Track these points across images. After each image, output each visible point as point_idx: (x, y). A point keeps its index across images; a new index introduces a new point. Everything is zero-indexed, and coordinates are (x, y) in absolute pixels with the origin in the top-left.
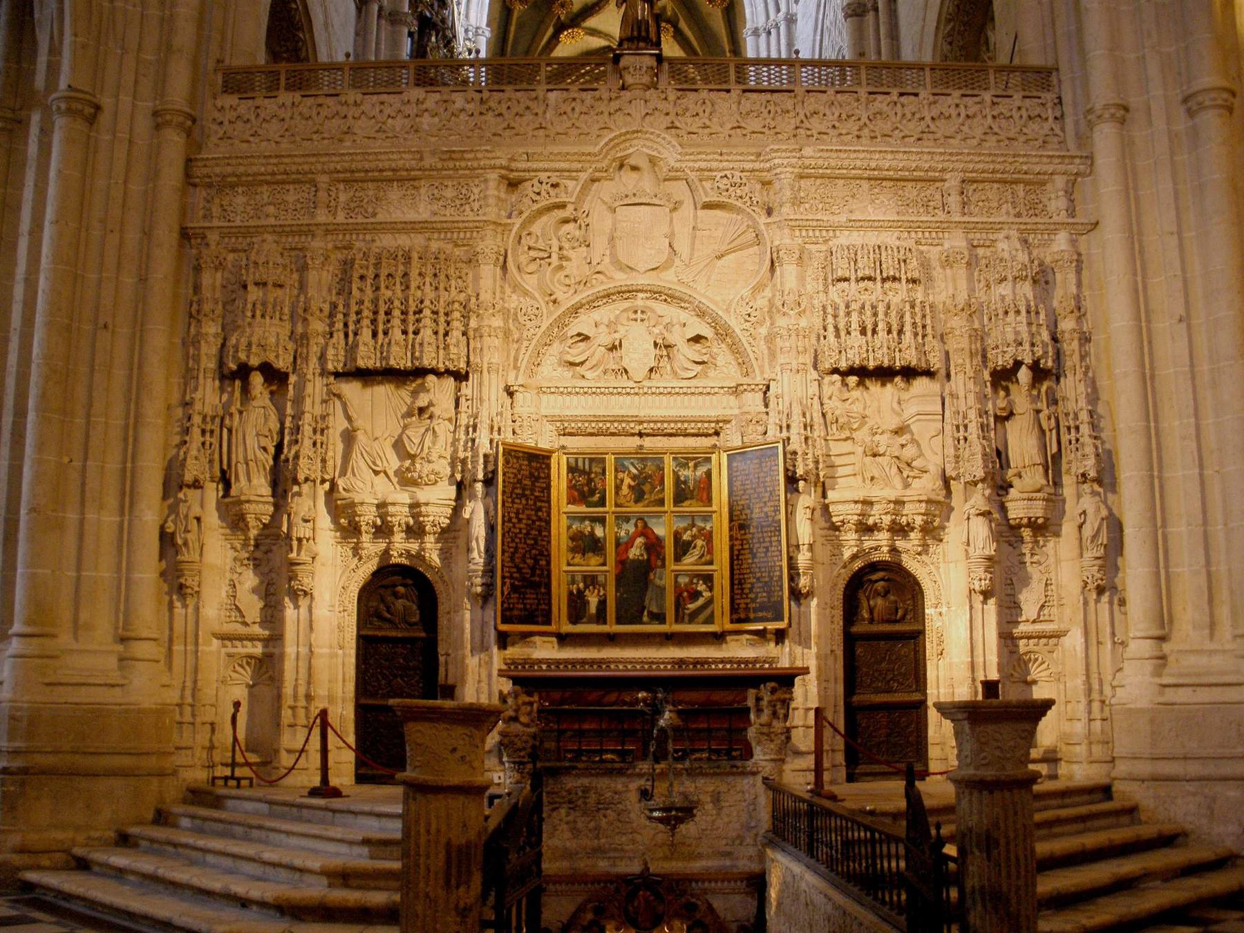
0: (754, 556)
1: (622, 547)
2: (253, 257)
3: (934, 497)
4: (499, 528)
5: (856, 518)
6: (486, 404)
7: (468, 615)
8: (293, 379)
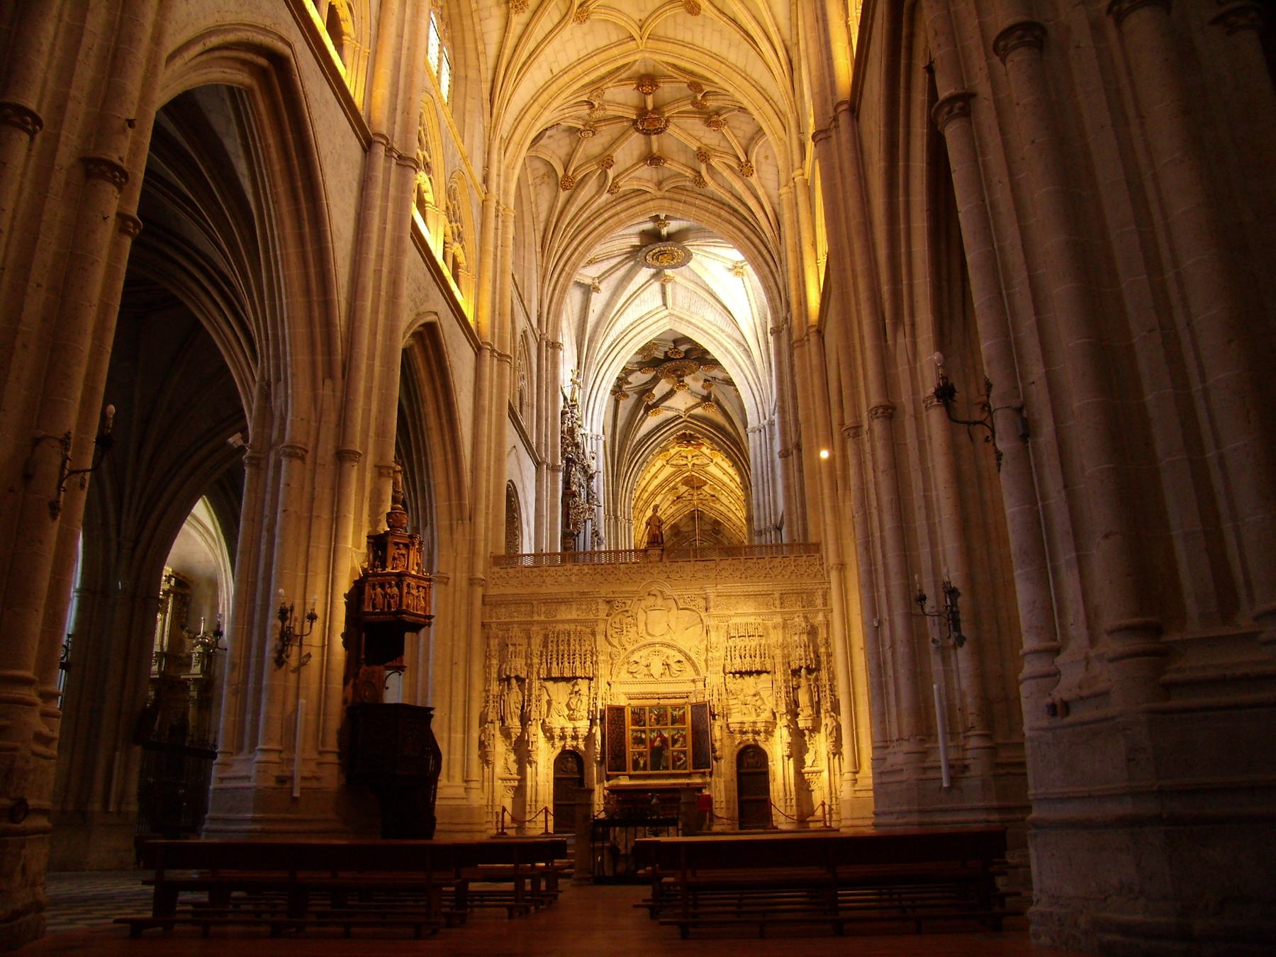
3: (768, 720)
8: (527, 681)
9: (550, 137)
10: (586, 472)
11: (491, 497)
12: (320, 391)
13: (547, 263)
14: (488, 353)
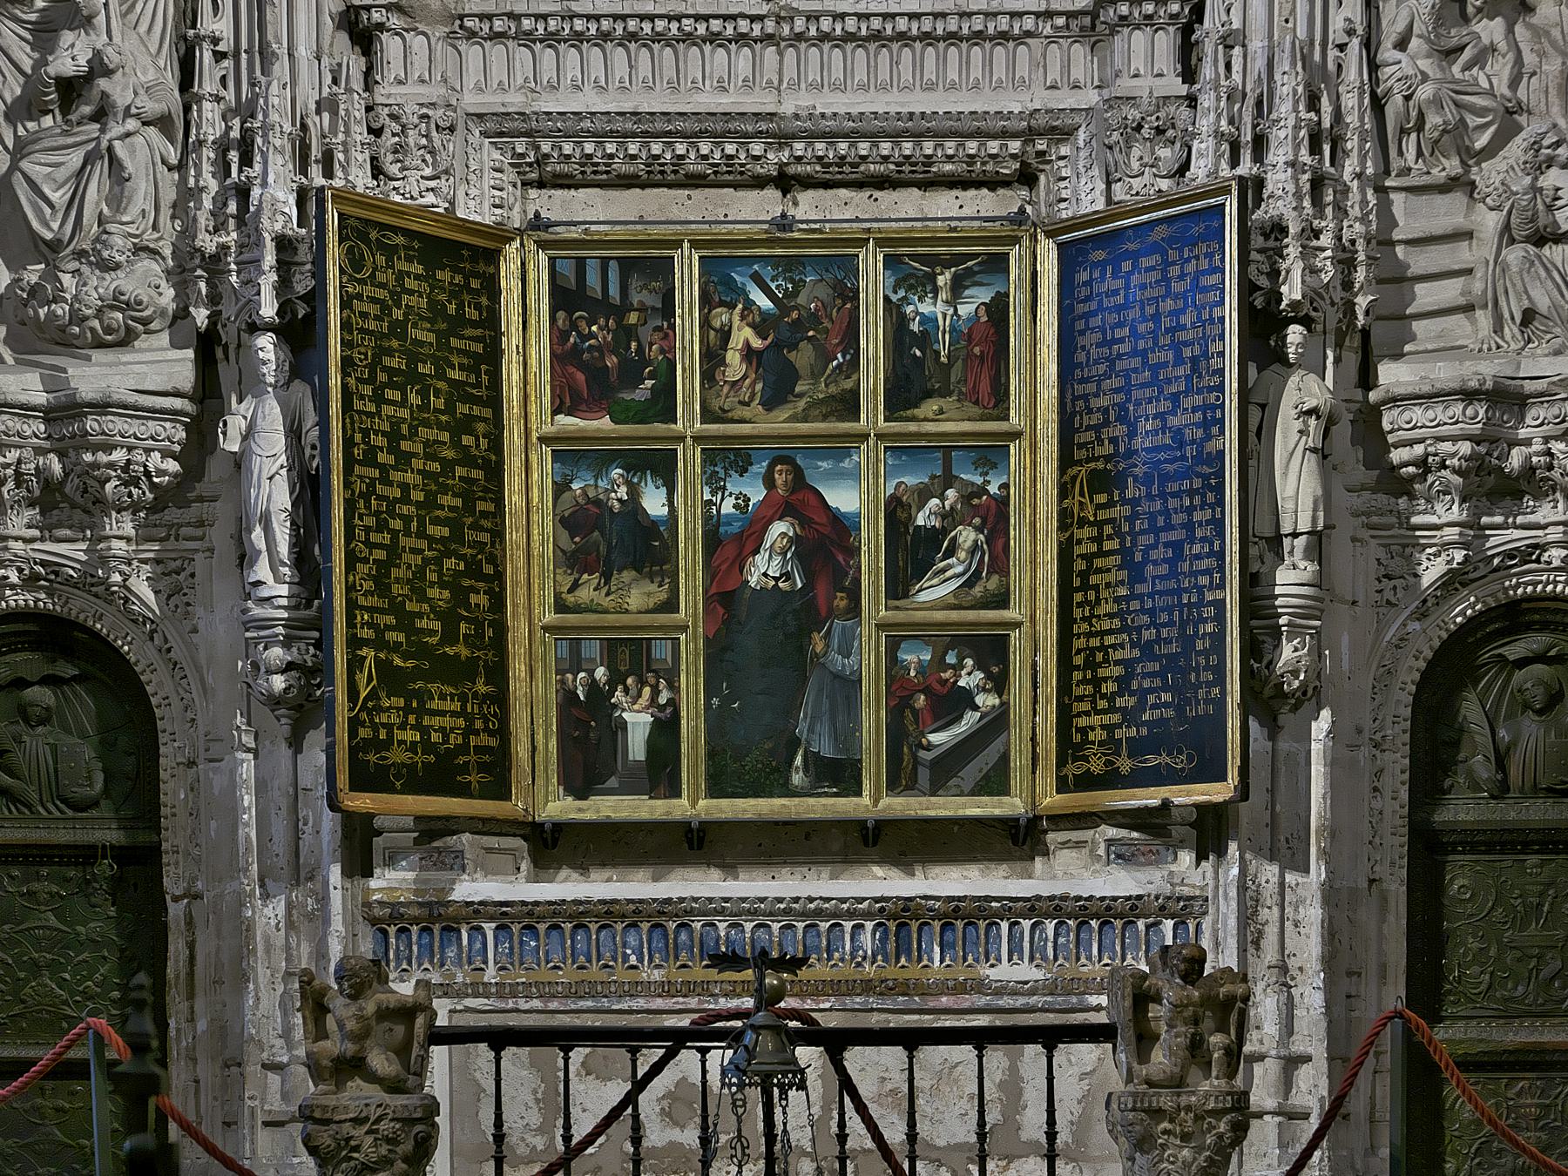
0: (1136, 575)
1: (729, 551)
4: (337, 481)
5: (1465, 448)
6: (281, 69)
7: (247, 768)
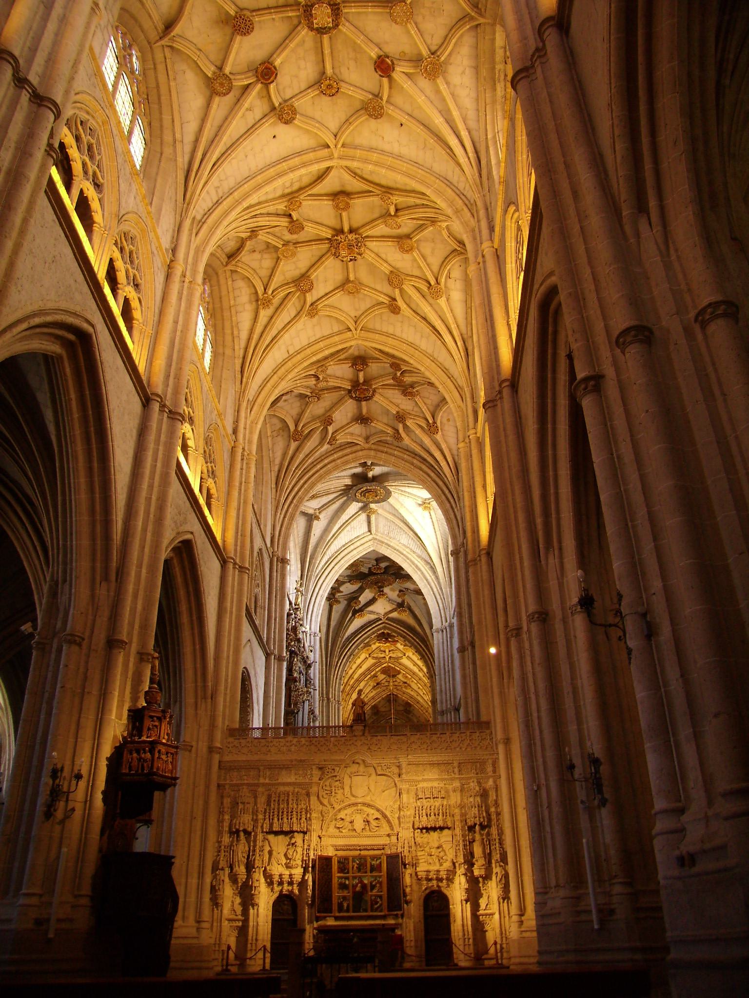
2: (240, 794)
8: (253, 834)
9: (285, 401)
10: (305, 662)
11: (229, 680)
12: (98, 591)
13: (280, 497)
14: (231, 566)
